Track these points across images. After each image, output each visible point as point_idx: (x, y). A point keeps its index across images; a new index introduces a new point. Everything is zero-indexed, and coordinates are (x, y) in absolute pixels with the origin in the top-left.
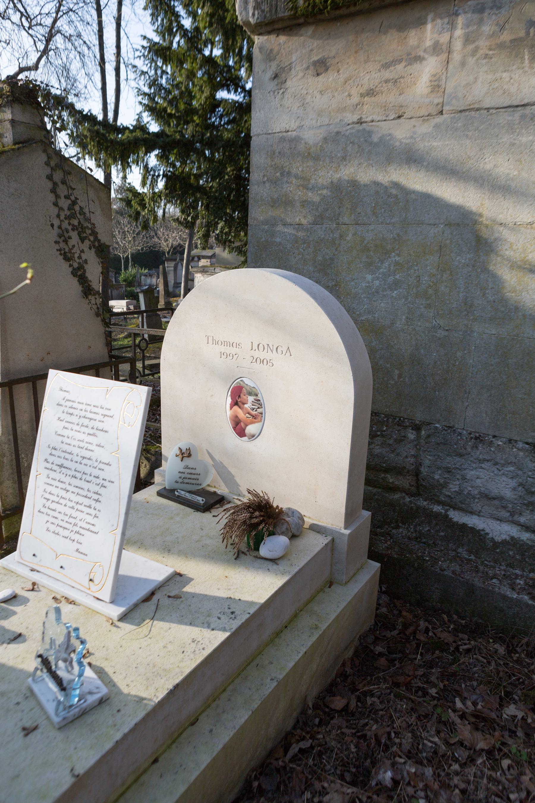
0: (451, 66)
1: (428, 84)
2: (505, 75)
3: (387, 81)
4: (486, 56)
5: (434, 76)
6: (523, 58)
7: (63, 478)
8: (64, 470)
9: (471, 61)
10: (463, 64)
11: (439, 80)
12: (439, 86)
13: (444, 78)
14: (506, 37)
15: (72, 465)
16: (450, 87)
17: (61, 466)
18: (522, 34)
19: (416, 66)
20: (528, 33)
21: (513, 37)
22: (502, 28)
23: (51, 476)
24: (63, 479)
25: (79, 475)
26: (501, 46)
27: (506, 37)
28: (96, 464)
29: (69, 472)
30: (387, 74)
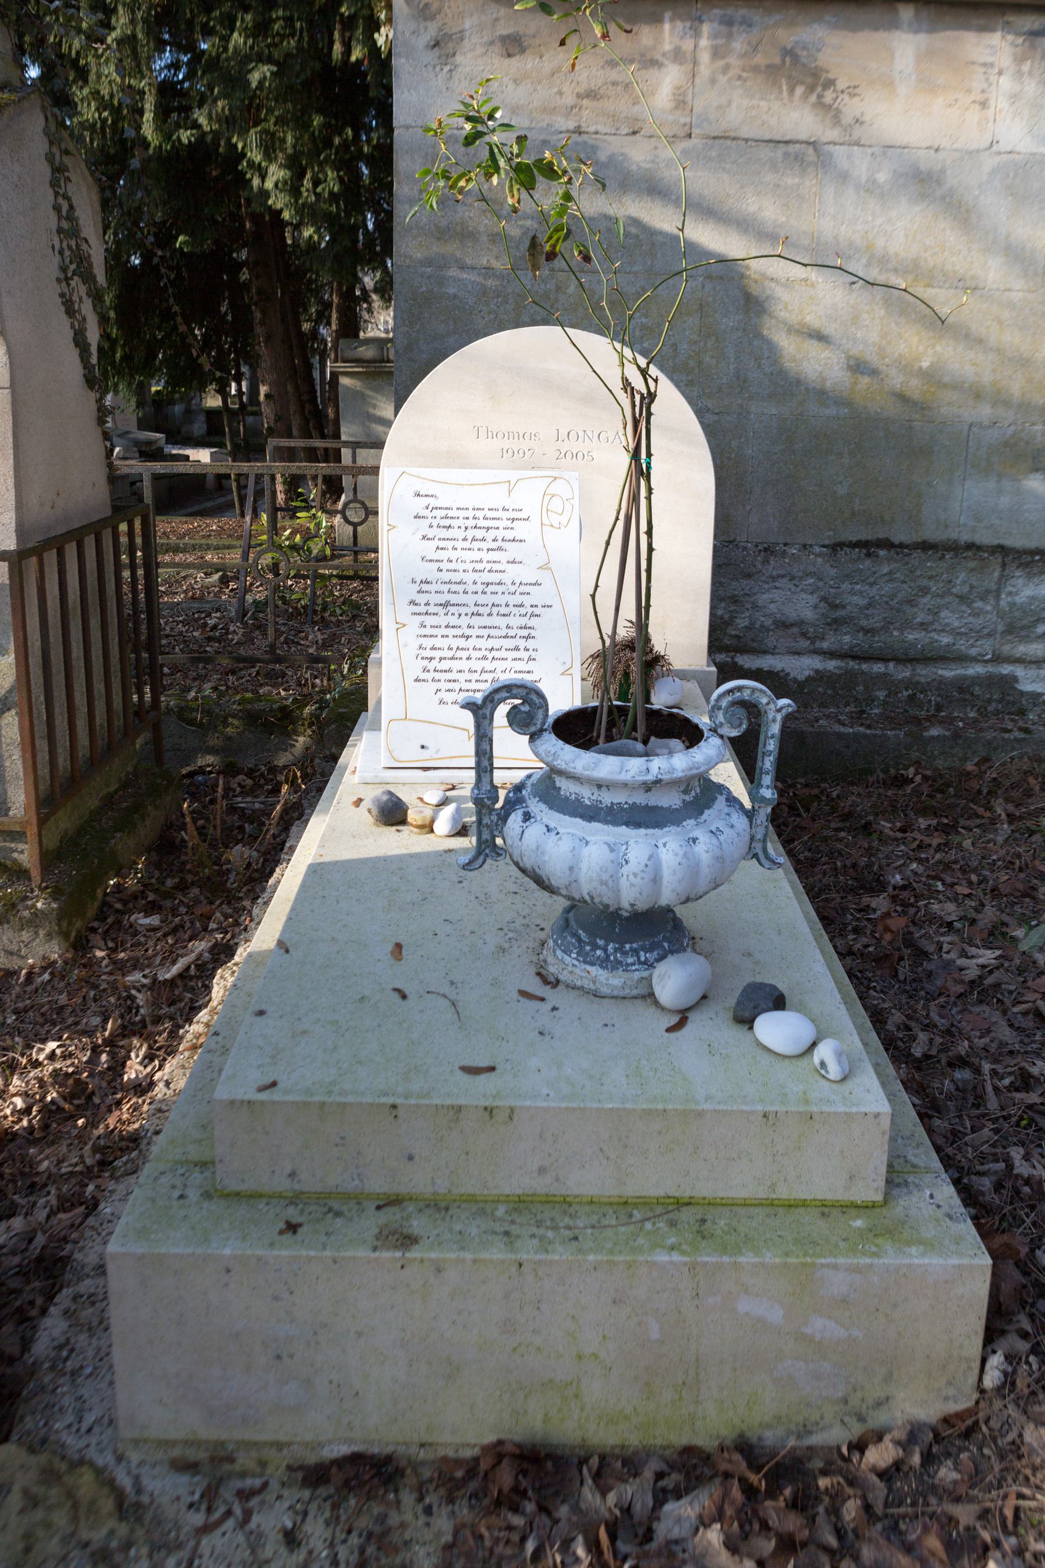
0: (698, 81)
1: (671, 97)
2: (762, 103)
3: (614, 84)
4: (740, 77)
5: (679, 88)
6: (780, 88)
7: (453, 620)
8: (452, 609)
9: (723, 80)
10: (713, 81)
11: (684, 94)
12: (685, 103)
13: (690, 92)
14: (759, 59)
15: (470, 599)
16: (699, 106)
17: (446, 605)
18: (777, 60)
19: (653, 73)
20: (784, 62)
21: (768, 62)
22: (755, 49)
23: (428, 623)
24: (453, 620)
25: (481, 610)
26: (755, 69)
27: (759, 59)
28: (512, 589)
29: (463, 610)
30: (613, 75)
